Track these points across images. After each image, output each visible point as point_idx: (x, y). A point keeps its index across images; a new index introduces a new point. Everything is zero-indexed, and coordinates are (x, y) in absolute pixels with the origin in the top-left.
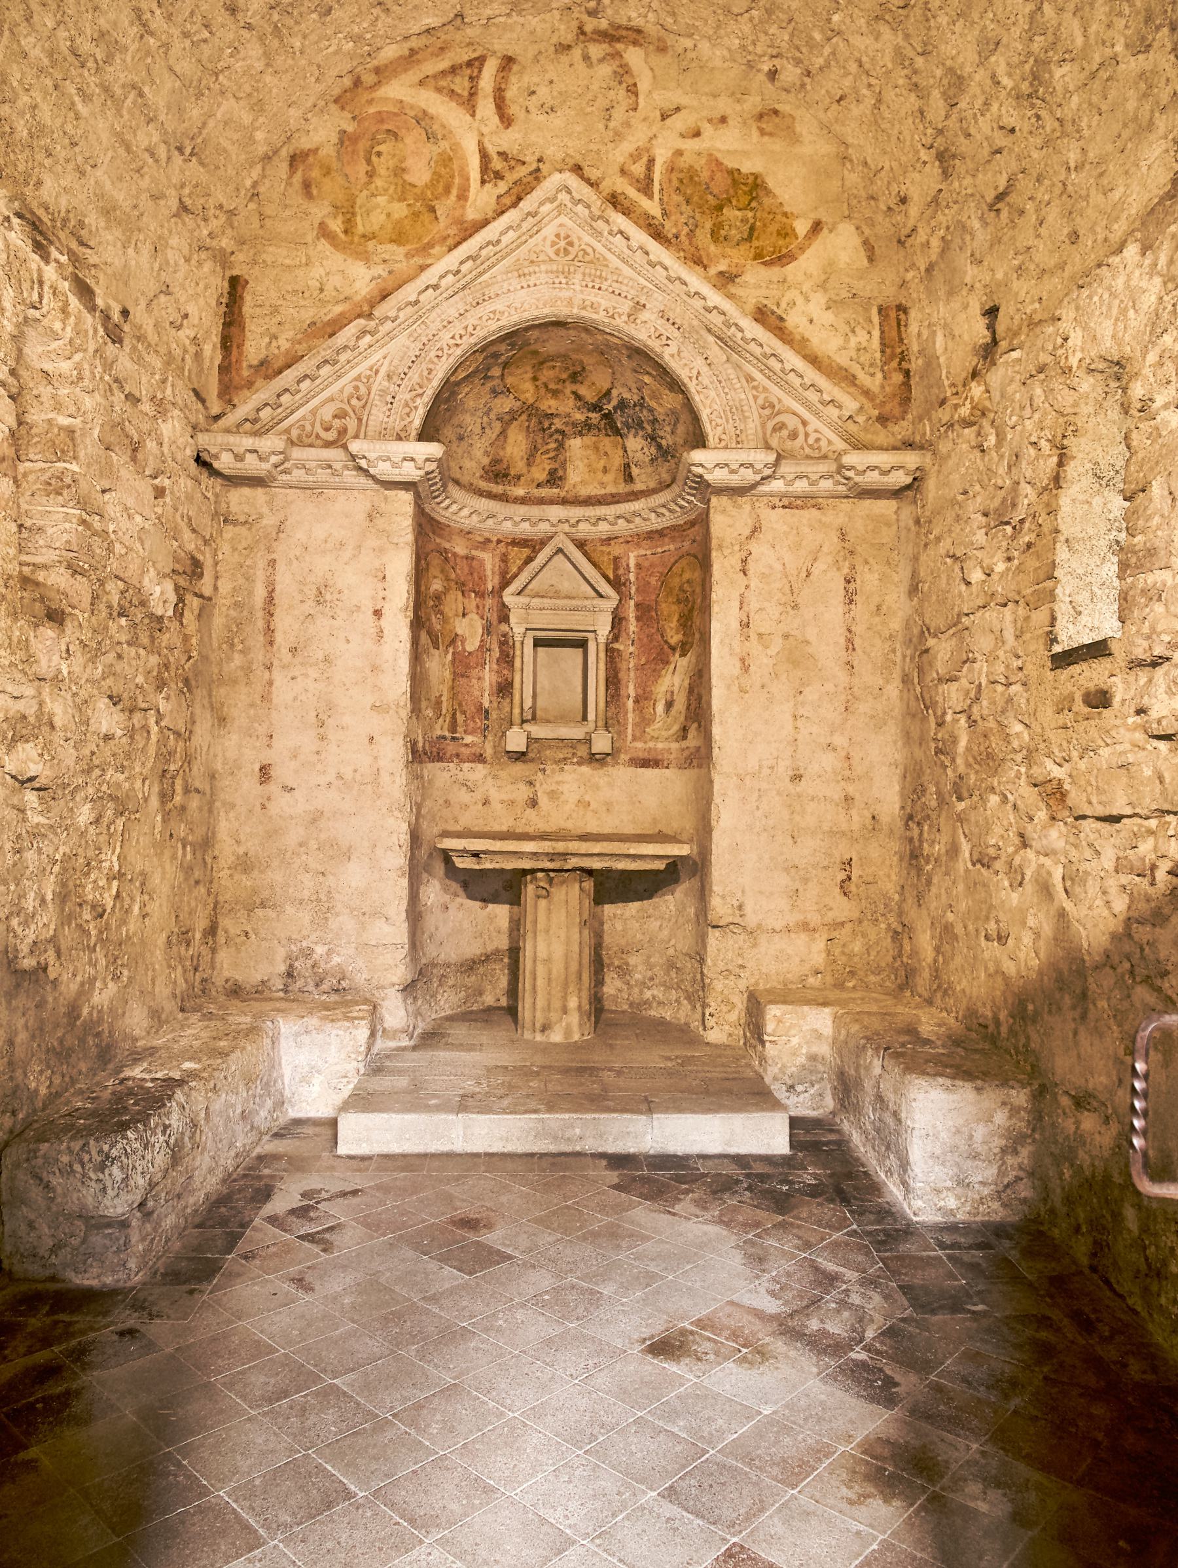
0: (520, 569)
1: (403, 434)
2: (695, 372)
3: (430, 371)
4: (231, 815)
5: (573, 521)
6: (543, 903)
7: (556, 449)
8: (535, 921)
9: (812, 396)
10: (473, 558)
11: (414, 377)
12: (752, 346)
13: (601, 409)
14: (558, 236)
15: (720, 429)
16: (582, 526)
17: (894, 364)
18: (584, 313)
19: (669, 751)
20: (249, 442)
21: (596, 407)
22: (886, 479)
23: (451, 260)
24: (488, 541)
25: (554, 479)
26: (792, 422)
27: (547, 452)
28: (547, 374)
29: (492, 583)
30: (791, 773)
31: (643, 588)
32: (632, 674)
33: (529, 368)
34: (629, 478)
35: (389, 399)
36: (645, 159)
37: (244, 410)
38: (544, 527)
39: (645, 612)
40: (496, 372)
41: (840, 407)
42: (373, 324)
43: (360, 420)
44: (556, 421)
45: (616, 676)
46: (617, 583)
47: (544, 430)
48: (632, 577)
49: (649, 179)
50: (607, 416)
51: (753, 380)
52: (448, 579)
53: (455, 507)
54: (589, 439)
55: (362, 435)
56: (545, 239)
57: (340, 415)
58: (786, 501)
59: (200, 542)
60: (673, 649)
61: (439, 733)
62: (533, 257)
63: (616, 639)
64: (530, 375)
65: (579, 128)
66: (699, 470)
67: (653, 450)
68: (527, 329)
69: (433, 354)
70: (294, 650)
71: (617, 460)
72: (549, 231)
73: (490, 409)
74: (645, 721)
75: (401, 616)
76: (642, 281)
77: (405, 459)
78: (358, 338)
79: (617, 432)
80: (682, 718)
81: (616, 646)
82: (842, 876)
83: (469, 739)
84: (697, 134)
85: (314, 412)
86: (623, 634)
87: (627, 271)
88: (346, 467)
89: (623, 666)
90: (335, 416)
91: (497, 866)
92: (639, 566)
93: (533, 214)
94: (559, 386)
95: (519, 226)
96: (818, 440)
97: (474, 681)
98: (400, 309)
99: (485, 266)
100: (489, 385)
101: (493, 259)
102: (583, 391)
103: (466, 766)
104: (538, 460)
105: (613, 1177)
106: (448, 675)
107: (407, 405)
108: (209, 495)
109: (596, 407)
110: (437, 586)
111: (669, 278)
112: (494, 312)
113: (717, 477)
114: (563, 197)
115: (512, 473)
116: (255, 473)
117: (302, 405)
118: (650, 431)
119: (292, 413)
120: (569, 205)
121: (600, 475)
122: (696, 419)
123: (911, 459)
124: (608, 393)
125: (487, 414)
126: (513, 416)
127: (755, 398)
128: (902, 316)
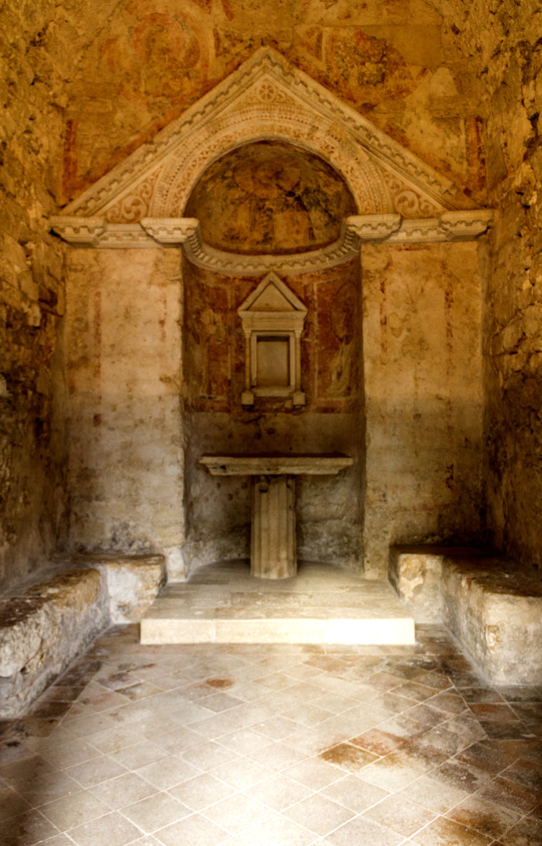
0: (248, 295)
1: (174, 214)
2: (350, 168)
3: (189, 175)
4: (78, 445)
5: (279, 264)
6: (264, 496)
7: (268, 221)
8: (260, 506)
9: (422, 179)
11: (180, 178)
12: (385, 150)
14: (264, 87)
15: (366, 203)
17: (476, 155)
18: (281, 135)
19: (340, 402)
20: (81, 221)
21: (291, 194)
22: (470, 228)
23: (198, 106)
24: (228, 278)
25: (267, 239)
26: (411, 196)
27: (262, 222)
28: (261, 174)
29: (230, 304)
30: (413, 413)
31: (322, 303)
32: (317, 357)
33: (249, 171)
34: (312, 236)
35: (165, 192)
36: (316, 34)
37: (78, 202)
38: (262, 269)
39: (324, 318)
40: (229, 174)
41: (440, 185)
42: (153, 147)
43: (148, 206)
45: (307, 358)
46: (306, 302)
47: (260, 209)
48: (315, 297)
49: (319, 47)
50: (298, 199)
51: (386, 171)
52: (204, 302)
53: (207, 258)
54: (287, 213)
55: (149, 215)
56: (255, 89)
57: (136, 203)
58: (408, 246)
59: (55, 283)
60: (341, 340)
61: (201, 394)
62: (249, 101)
63: (306, 335)
64: (249, 176)
65: (275, 17)
66: (352, 229)
67: (326, 219)
68: (247, 147)
69: (190, 164)
70: (113, 346)
71: (305, 225)
72: (258, 84)
74: (324, 386)
75: (176, 324)
76: (316, 112)
77: (175, 229)
78: (145, 156)
79: (304, 208)
80: (347, 382)
81: (307, 340)
82: (448, 475)
83: (219, 398)
84: (348, 16)
85: (120, 202)
86: (311, 332)
87: (306, 106)
88: (140, 235)
89: (311, 351)
90: (134, 204)
91: (236, 473)
92: (319, 290)
93: (248, 74)
95: (240, 81)
96: (427, 207)
97: (222, 364)
98: (169, 137)
99: (219, 108)
100: (226, 182)
101: (225, 104)
102: (282, 184)
103: (218, 414)
104: (257, 228)
105: (307, 657)
106: (206, 359)
107: (175, 196)
108: (60, 254)
109: (291, 194)
110: (197, 306)
111: (332, 110)
112: (226, 137)
113: (364, 232)
114: (266, 62)
115: (242, 236)
116: (85, 240)
117: (113, 198)
119: (108, 202)
120: (270, 67)
121: (295, 235)
122: (351, 197)
123: (484, 215)
124: (298, 185)
125: (225, 200)
126: (241, 201)
127: (387, 182)
128: (480, 125)
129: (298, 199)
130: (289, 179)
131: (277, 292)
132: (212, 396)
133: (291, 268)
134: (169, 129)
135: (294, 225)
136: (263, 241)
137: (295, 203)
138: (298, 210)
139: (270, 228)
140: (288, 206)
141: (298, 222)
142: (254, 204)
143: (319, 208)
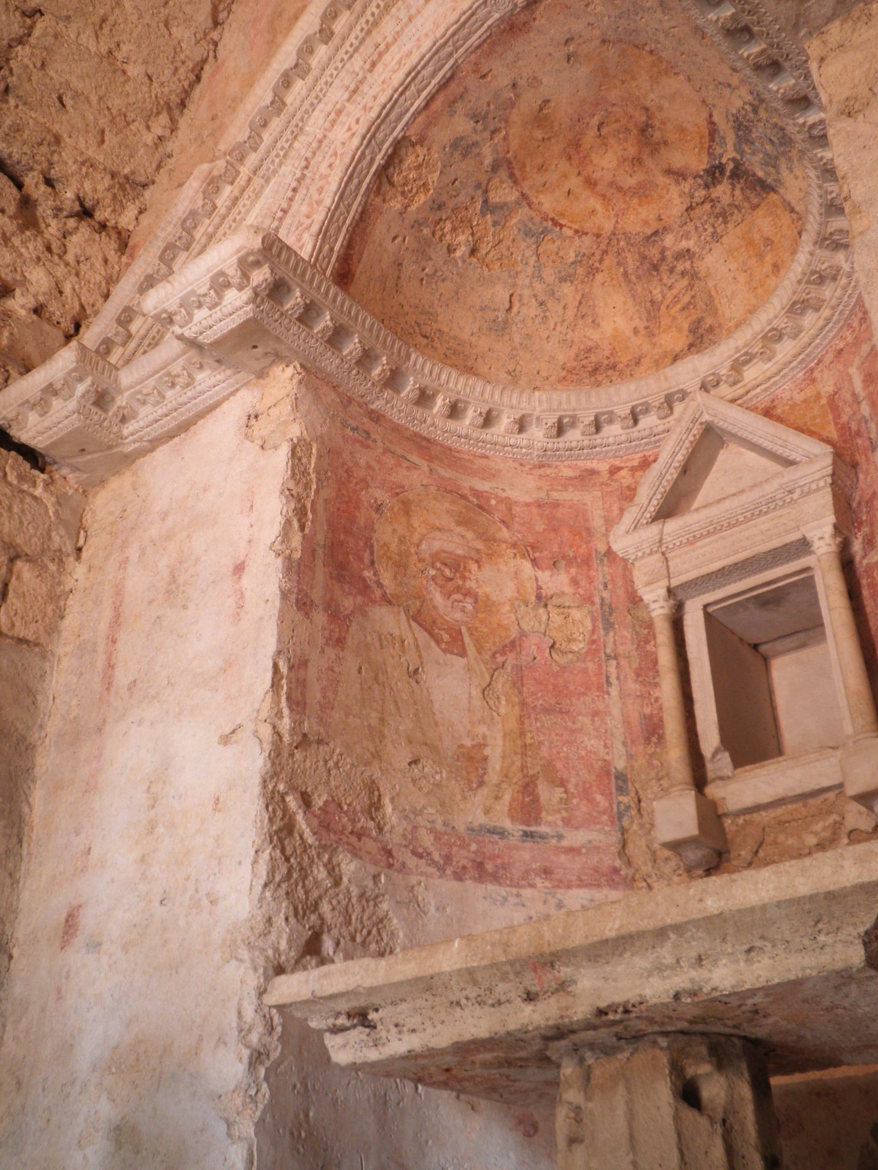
7: (691, 286)
10: (556, 505)
13: (721, 168)
21: (715, 173)
27: (676, 299)
33: (564, 165)
44: (669, 240)
47: (655, 267)
54: (732, 236)
61: (480, 819)
64: (574, 182)
79: (764, 187)
83: (577, 838)
94: (639, 177)
102: (678, 159)
104: (665, 321)
125: (538, 275)
129: (738, 173)
130: (682, 130)
131: (751, 457)
132: (543, 829)
133: (769, 367)
134: (249, 107)
135: (760, 256)
136: (691, 346)
137: (738, 192)
138: (755, 207)
139: (701, 304)
140: (724, 216)
141: (768, 241)
142: (632, 262)
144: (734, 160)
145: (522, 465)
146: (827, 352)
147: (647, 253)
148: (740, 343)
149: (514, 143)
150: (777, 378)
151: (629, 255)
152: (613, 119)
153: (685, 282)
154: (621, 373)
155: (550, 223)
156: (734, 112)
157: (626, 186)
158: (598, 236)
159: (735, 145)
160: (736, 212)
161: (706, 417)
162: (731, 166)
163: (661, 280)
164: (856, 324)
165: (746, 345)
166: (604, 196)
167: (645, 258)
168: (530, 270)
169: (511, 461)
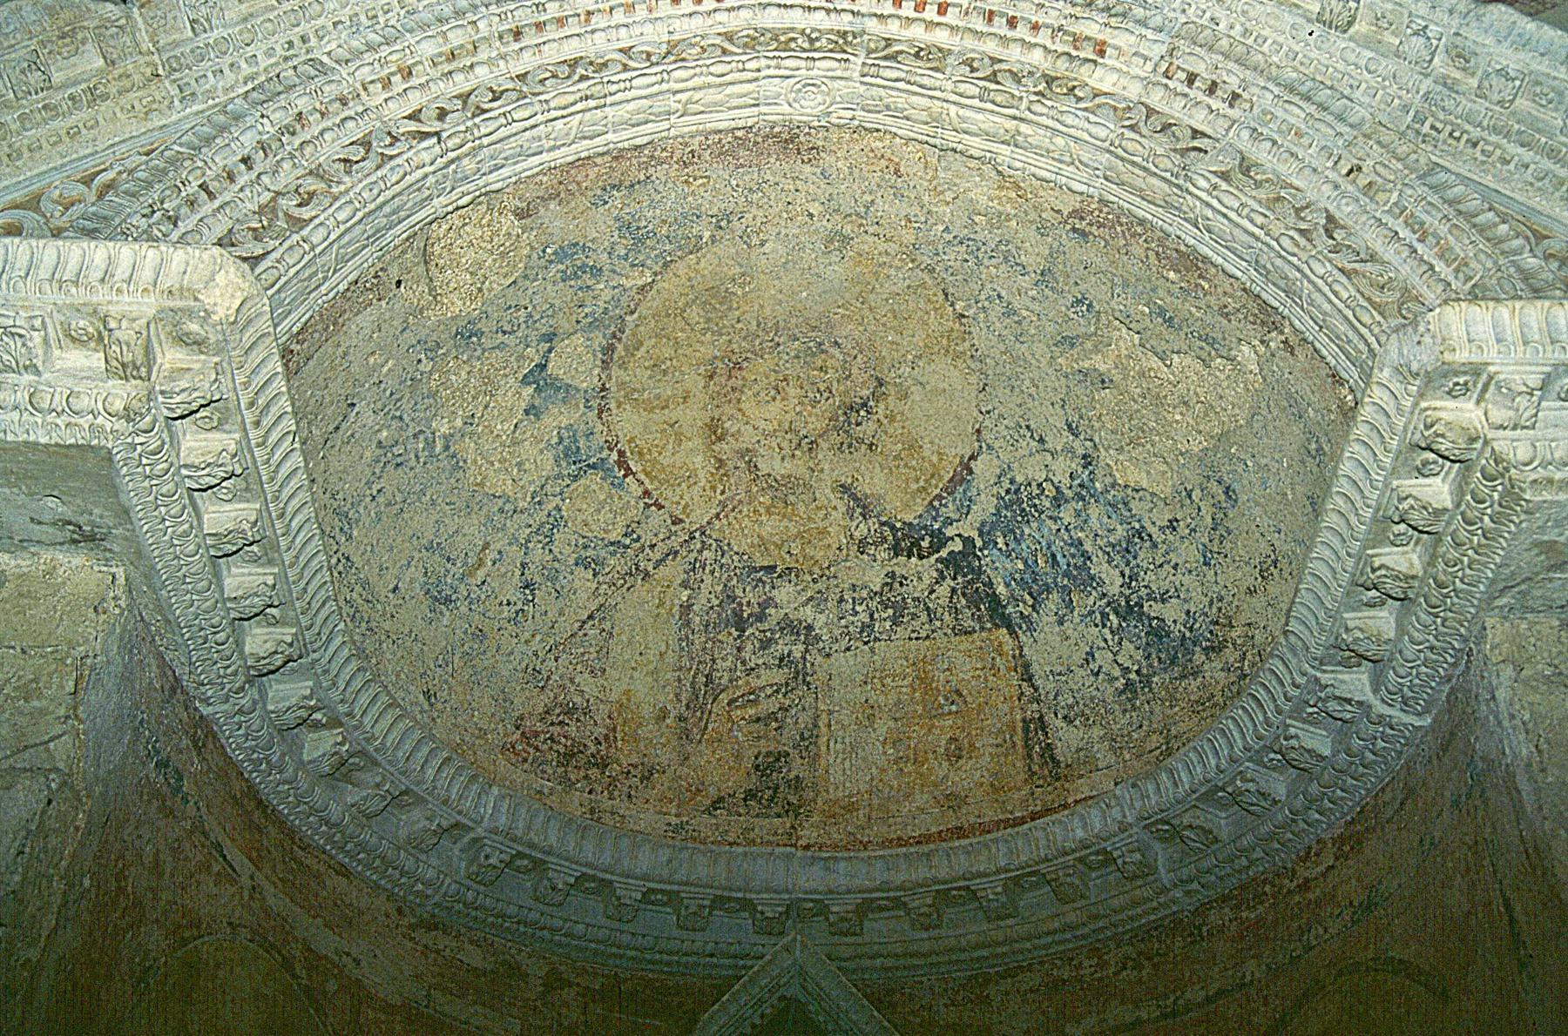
7: (786, 688)
13: (940, 541)
16: (877, 928)
24: (515, 971)
44: (784, 593)
50: (962, 563)
64: (692, 416)
67: (1130, 654)
73: (557, 521)
94: (797, 467)
100: (558, 418)
102: (873, 481)
115: (626, 755)
118: (1113, 583)
130: (913, 447)
136: (750, 795)
137: (943, 590)
139: (791, 733)
143: (1089, 601)
144: (968, 541)
145: (400, 911)
146: (1030, 967)
147: (739, 592)
148: (899, 878)
149: (652, 302)
150: (922, 962)
151: (708, 580)
152: (819, 363)
153: (779, 676)
154: (612, 783)
155: (615, 456)
156: (1019, 479)
157: (764, 468)
158: (677, 521)
159: (983, 524)
160: (924, 617)
161: (794, 991)
162: (957, 546)
163: (739, 649)
164: (1112, 958)
165: (901, 888)
166: (721, 463)
167: (732, 598)
168: (541, 516)
169: (383, 897)
